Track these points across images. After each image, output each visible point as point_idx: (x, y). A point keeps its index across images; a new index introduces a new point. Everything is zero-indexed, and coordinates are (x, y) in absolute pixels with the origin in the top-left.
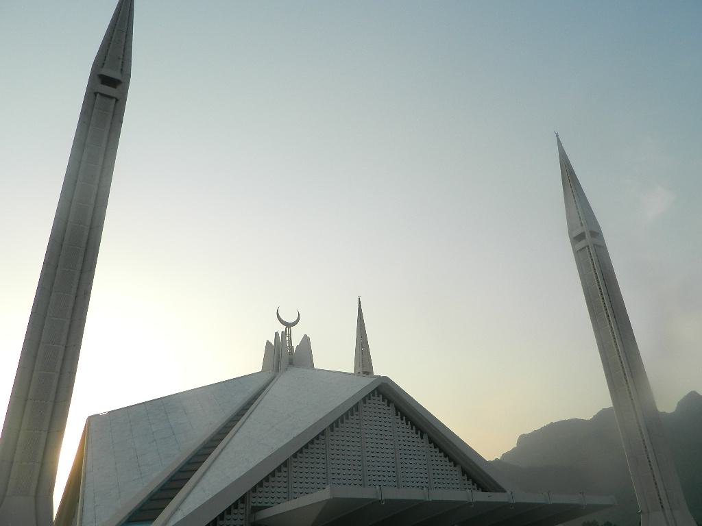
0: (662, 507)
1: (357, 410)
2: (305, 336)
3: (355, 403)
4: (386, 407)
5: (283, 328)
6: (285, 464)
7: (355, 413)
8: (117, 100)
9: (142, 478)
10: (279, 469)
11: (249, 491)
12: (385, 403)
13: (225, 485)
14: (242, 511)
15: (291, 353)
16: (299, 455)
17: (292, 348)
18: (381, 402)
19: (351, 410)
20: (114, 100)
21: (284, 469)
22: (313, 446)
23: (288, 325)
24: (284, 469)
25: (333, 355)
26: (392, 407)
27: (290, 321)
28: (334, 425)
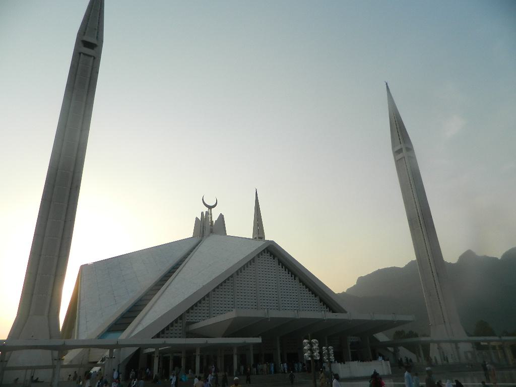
0: (445, 322)
2: (221, 214)
3: (252, 258)
4: (272, 260)
5: (207, 209)
6: (208, 295)
7: (252, 263)
8: (94, 58)
10: (204, 299)
11: (185, 312)
12: (272, 258)
13: (169, 309)
14: (181, 325)
16: (216, 290)
17: (212, 222)
20: (93, 58)
21: (207, 299)
22: (227, 283)
23: (210, 208)
24: (207, 299)
25: (239, 227)
28: (239, 271)
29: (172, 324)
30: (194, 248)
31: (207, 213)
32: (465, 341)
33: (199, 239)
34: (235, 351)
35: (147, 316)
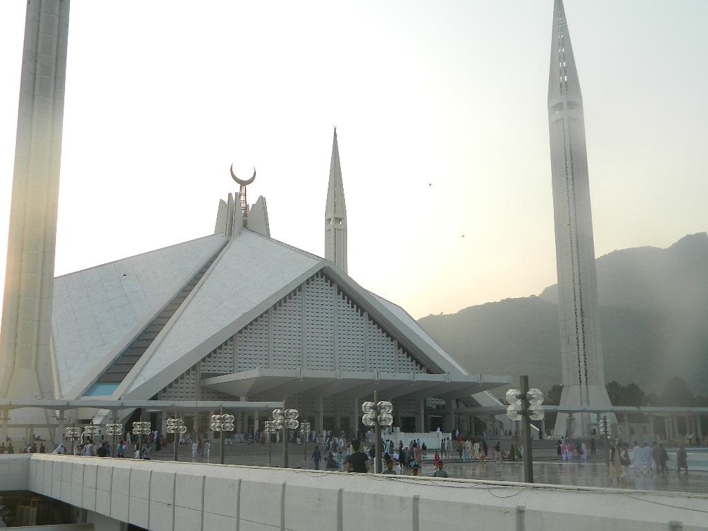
1: (300, 291)
4: (328, 287)
5: (236, 188)
6: (231, 339)
7: (298, 293)
9: (104, 344)
10: (226, 343)
12: (329, 284)
15: (245, 215)
18: (324, 283)
19: (294, 291)
21: (229, 343)
23: (243, 184)
24: (229, 343)
26: (335, 287)
27: (245, 178)
29: (182, 377)
30: (216, 256)
31: (238, 196)
32: (611, 411)
33: (224, 240)
34: (257, 416)
35: (148, 366)
